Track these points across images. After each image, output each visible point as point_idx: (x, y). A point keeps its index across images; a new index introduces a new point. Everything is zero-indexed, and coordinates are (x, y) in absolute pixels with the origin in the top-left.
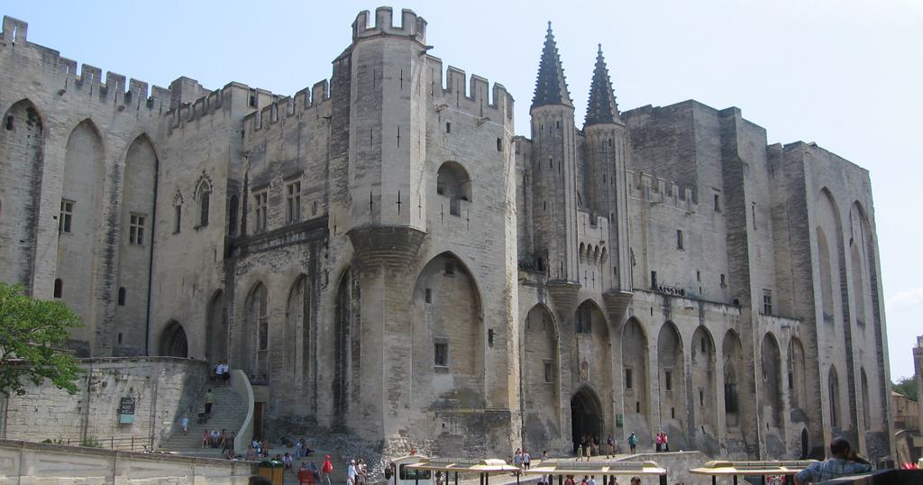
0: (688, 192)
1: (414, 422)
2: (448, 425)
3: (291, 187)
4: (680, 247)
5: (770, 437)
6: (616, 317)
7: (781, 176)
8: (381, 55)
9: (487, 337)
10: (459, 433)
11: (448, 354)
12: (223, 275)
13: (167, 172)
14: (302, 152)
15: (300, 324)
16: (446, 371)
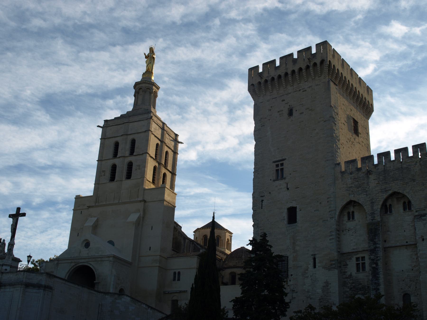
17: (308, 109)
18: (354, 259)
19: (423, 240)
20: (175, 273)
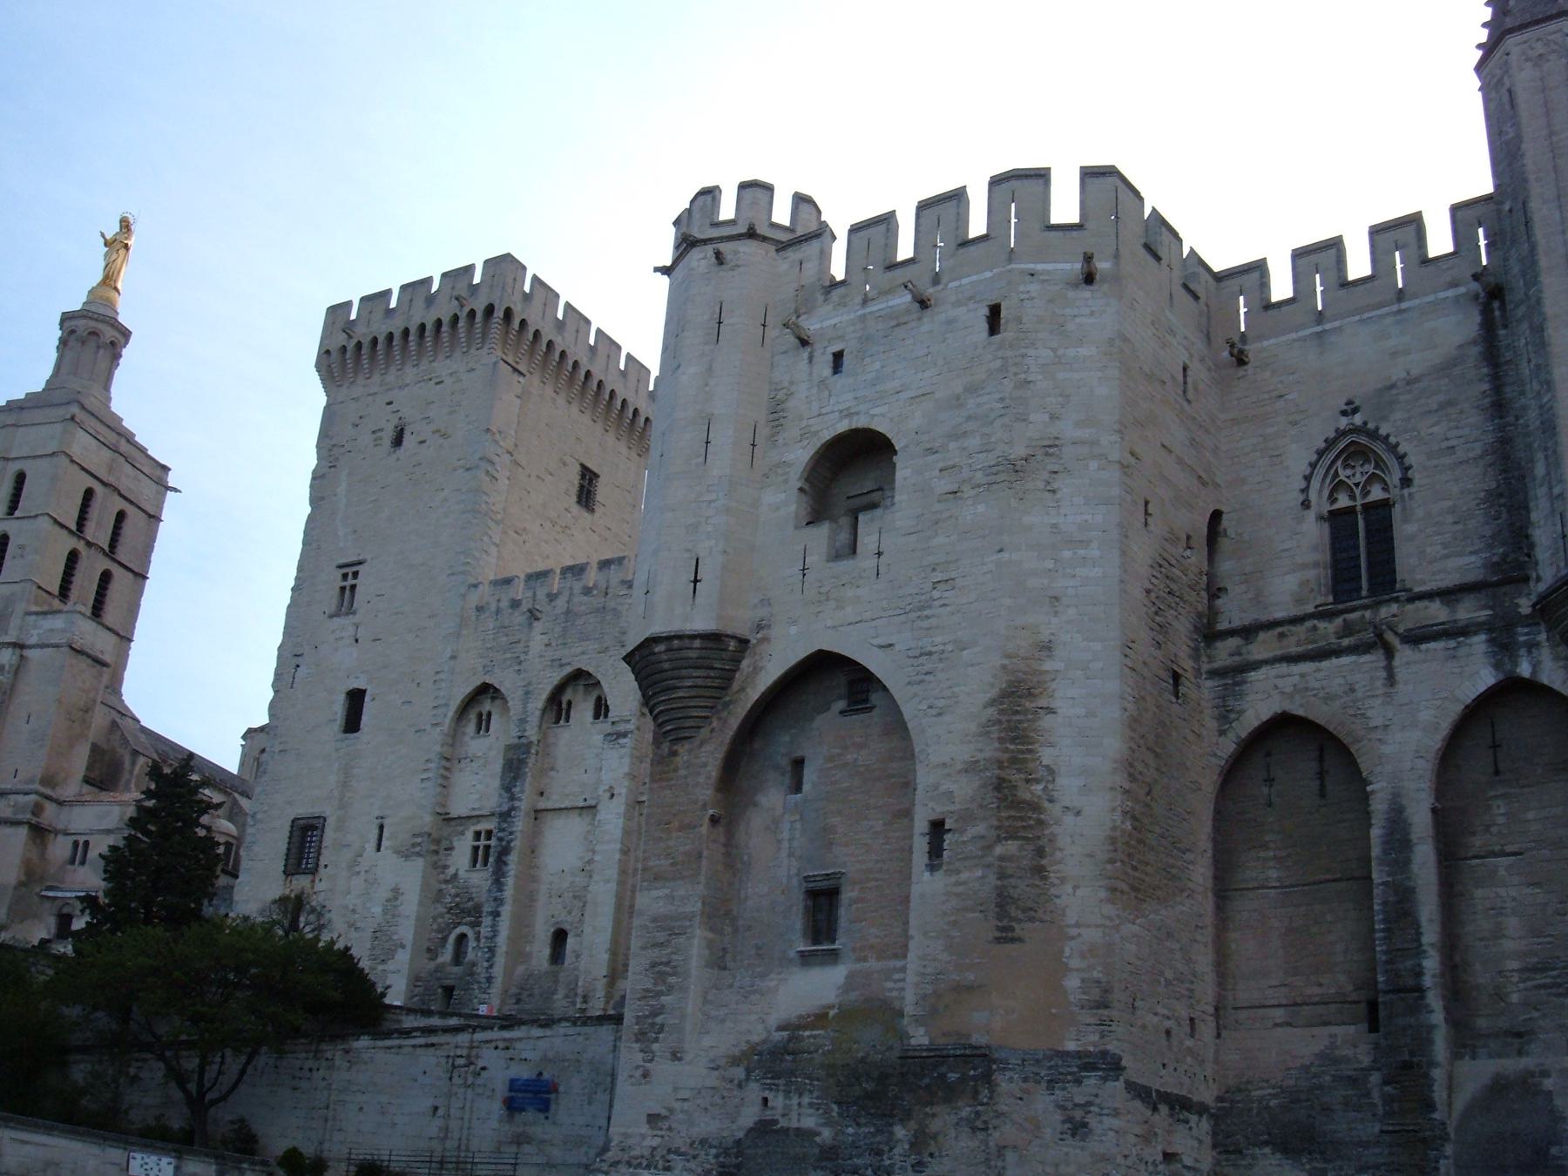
1: (686, 1095)
2: (777, 1101)
9: (921, 845)
10: (809, 1122)
11: (842, 911)
16: (833, 957)
17: (438, 431)
18: (470, 835)
19: (613, 795)
20: (76, 844)
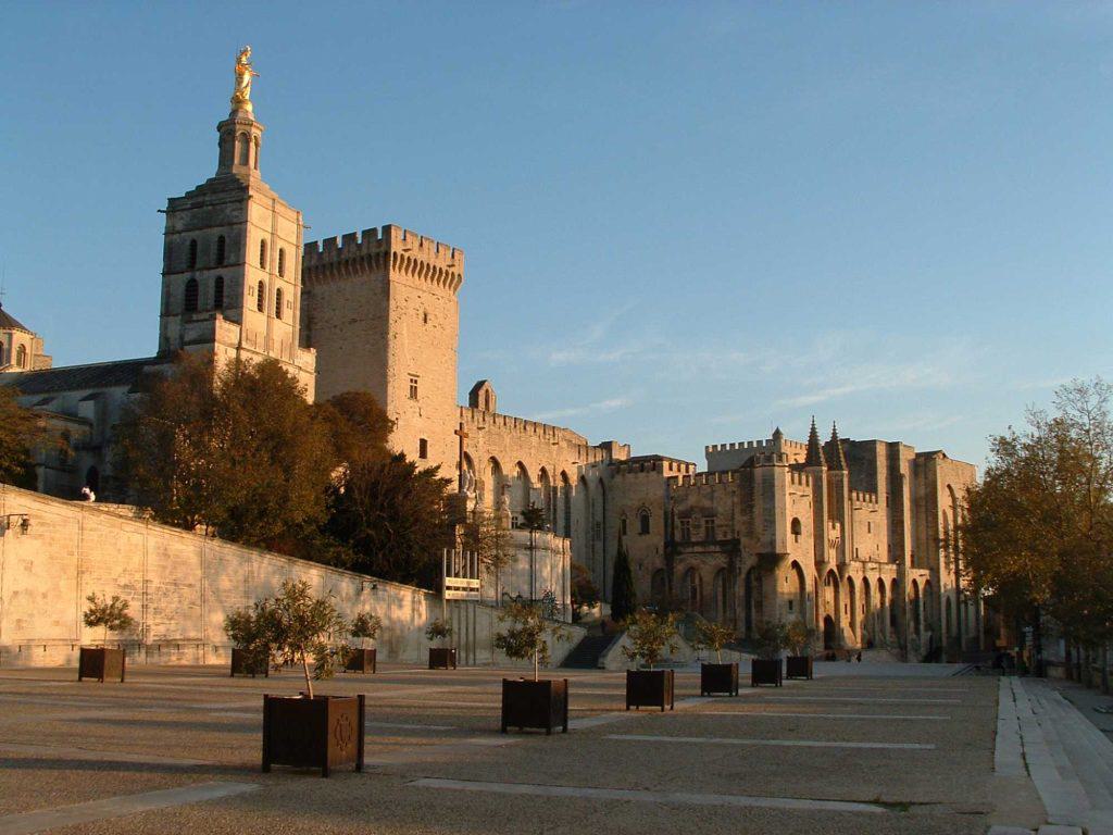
0: (873, 497)
3: (707, 522)
4: (869, 532)
5: (913, 640)
6: (841, 577)
7: (922, 480)
8: (773, 475)
12: (665, 562)
13: (613, 499)
14: (715, 505)
15: (720, 589)
